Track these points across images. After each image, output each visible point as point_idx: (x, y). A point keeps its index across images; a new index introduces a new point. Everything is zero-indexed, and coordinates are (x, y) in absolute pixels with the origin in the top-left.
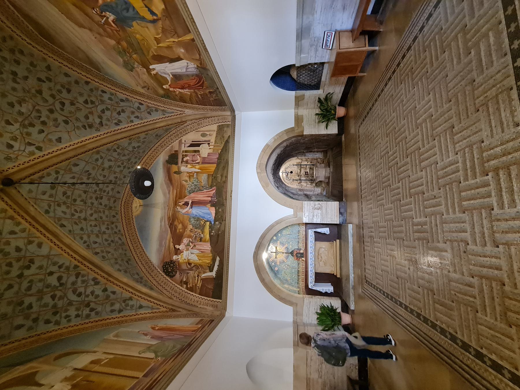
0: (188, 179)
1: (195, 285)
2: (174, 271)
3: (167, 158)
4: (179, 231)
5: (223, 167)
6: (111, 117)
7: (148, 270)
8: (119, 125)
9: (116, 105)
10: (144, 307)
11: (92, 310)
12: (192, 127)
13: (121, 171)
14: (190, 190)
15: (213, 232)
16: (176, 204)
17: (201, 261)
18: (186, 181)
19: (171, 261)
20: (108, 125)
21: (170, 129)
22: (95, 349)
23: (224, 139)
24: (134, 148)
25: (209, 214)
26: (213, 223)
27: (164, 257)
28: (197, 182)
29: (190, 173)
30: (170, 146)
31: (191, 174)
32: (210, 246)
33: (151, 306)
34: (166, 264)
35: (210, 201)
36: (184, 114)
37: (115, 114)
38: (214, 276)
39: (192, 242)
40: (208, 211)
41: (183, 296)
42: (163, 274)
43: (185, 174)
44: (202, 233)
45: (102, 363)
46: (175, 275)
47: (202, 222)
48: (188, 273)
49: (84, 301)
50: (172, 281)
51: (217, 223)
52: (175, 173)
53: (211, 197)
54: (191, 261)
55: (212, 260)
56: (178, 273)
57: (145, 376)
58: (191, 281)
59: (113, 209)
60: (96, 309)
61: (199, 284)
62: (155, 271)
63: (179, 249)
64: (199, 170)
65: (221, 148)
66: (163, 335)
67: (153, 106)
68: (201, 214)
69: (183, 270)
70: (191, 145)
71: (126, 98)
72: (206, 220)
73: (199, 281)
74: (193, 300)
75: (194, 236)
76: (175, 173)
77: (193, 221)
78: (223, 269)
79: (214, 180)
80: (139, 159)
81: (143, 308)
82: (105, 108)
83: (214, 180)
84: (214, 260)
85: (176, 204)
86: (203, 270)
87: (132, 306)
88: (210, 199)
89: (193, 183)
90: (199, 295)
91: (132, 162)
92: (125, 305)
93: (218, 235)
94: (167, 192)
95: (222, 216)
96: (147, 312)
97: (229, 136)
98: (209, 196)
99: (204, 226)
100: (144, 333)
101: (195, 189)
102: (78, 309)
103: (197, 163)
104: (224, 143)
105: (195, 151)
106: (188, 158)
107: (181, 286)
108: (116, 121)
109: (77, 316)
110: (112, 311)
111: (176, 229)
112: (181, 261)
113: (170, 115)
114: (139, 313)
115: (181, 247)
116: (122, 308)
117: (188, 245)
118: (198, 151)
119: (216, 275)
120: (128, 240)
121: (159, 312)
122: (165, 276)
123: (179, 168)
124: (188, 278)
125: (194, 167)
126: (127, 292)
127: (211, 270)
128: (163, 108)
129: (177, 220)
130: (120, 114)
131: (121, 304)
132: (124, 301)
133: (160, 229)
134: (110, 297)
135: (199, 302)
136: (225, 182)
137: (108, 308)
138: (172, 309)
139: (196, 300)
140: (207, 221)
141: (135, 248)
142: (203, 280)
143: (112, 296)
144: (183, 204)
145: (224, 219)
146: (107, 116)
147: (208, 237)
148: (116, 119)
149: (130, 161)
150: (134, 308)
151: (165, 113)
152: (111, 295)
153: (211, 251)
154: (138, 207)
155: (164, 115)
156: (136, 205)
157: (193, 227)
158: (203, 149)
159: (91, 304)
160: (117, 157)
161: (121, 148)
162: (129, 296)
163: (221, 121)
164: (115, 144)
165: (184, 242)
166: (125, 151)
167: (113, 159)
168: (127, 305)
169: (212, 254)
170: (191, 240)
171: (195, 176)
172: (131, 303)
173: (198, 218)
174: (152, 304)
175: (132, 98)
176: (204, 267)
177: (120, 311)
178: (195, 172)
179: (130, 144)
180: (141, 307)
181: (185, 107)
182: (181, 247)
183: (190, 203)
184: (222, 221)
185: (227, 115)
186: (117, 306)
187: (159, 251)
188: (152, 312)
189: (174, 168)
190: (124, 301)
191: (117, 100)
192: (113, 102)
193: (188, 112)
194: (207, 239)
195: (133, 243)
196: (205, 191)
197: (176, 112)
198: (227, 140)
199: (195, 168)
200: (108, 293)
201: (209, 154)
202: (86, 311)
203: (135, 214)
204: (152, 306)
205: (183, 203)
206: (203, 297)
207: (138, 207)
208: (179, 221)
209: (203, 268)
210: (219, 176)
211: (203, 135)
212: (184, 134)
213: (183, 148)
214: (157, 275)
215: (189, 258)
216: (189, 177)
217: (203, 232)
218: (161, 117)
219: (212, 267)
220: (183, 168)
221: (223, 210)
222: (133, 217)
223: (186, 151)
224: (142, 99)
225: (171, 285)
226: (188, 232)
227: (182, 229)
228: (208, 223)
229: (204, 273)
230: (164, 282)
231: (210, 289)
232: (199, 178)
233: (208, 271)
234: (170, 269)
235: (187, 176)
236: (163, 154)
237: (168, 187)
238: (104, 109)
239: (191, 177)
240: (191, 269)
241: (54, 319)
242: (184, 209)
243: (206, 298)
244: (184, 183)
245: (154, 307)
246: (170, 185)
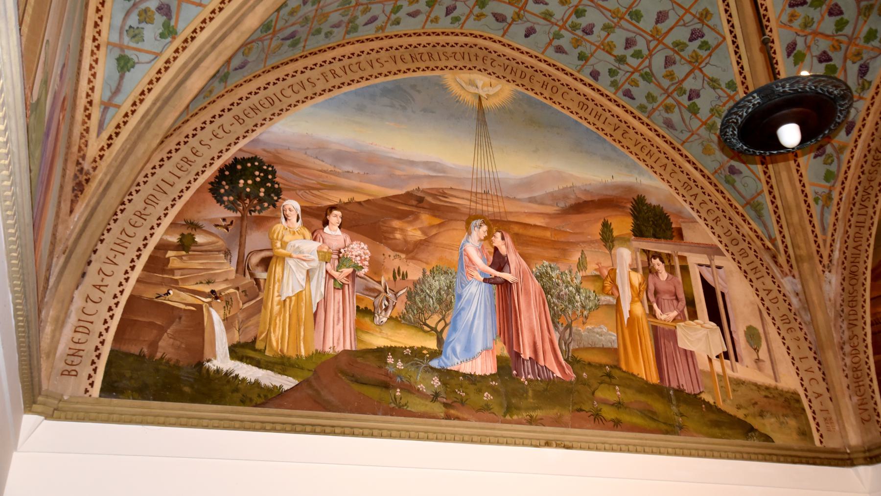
0: (591, 270)
1: (176, 281)
2: (239, 198)
3: (652, 201)
4: (395, 229)
5: (654, 413)
6: (815, 33)
7: (245, 104)
8: (789, 55)
9: (853, 49)
10: (122, 77)
12: (772, 295)
13: (609, 49)
14: (551, 278)
15: (400, 365)
16: (496, 224)
17: (276, 308)
18: (582, 265)
19: (278, 192)
20: (791, 21)
21: (760, 216)
23: (754, 416)
24: (694, 95)
25: (468, 347)
26: (435, 363)
27: (298, 166)
28: (584, 307)
29: (613, 281)
30: (695, 215)
31: (608, 284)
32: (340, 349)
33: (117, 100)
34: (266, 172)
35: (518, 355)
36: (820, 268)
37: (823, 45)
38: (213, 365)
39: (353, 276)
40: (479, 347)
41: (130, 230)
42: (227, 157)
43: (606, 263)
44: (391, 318)
46: (220, 201)
47: (436, 318)
48: (227, 253)
50: (198, 191)
51: (436, 382)
52: (606, 226)
53: (534, 361)
54: (279, 269)
55: (283, 357)
56: (230, 214)
58: (195, 264)
59: (477, 10)
61: (178, 299)
62: (240, 130)
63: (326, 223)
64: (626, 315)
65: (721, 405)
67: (844, 167)
68: (467, 316)
69: (242, 237)
70: (709, 290)
71: (870, 83)
72: (444, 336)
73: (190, 299)
74: (108, 269)
75: (377, 287)
76: (606, 226)
77: (436, 284)
78: (243, 402)
79: (599, 373)
80: (642, 108)
81: (117, 75)
82: (846, 16)
83: (599, 373)
84: (281, 365)
85: (496, 224)
86: (241, 316)
87: (136, 34)
88: (527, 353)
89: (578, 290)
90: (131, 298)
91: (637, 85)
92: (146, 11)
93: (386, 386)
94: (535, 194)
95: (462, 402)
96: (98, 83)
97: (768, 438)
98: (535, 351)
99: (419, 325)
101: (559, 297)
103: (651, 308)
104: (740, 414)
105: (691, 303)
106: (664, 275)
107: (173, 224)
108: (800, 46)
111: (402, 216)
112: (279, 228)
113: (816, 221)
114: (101, 54)
115: (334, 233)
117: (342, 260)
118: (693, 316)
119: (218, 371)
120: (358, 45)
121: (87, 130)
122: (218, 164)
123: (624, 241)
124: (206, 251)
125: (637, 295)
126: (197, 23)
127: (237, 352)
128: (835, 196)
129: (437, 221)
130: (820, 61)
133: (400, 161)
135: (96, 294)
136: (597, 419)
138: (87, 181)
139: (107, 281)
140: (440, 341)
141: (327, 67)
142: (197, 316)
144: (496, 249)
145: (452, 412)
146: (819, 22)
147: (378, 341)
148: (809, 47)
149: (640, 79)
150: (126, 40)
151: (820, 203)
153: (319, 354)
154: (472, 90)
155: (816, 200)
156: (480, 84)
157: (415, 284)
158: (704, 332)
160: (669, 40)
161: (703, 53)
162: (180, 27)
163: (816, 405)
164: (724, 38)
165: (355, 245)
166: (687, 68)
167: (663, 27)
168: (145, 16)
169: (309, 358)
170: (362, 273)
171: (605, 299)
172: (151, 32)
173: (449, 306)
174: (126, 107)
175: (868, 103)
176: (253, 321)
178: (618, 300)
179: (714, 83)
180: (124, 64)
181: (851, 277)
182: (334, 233)
183: (504, 275)
184: (446, 405)
185: (843, 428)
187: (320, 149)
188: (90, 103)
189: (622, 225)
191: (865, 56)
192: (861, 42)
193: (832, 283)
194: (366, 338)
195: (346, 61)
196: (556, 337)
197: (825, 241)
198: (752, 429)
199: (633, 302)
201: (689, 355)
203: (448, 77)
205: (503, 250)
206: (118, 312)
207: (472, 90)
208: (434, 232)
209: (248, 317)
210: (615, 394)
211: (752, 335)
212: (744, 267)
213: (694, 259)
214: (221, 133)
215: (290, 262)
216: (598, 278)
217: (396, 321)
218: (808, 189)
219: (251, 354)
220: (625, 255)
221: (486, 408)
222: (437, 73)
223: (685, 269)
224: (865, 133)
225: (182, 185)
226: (394, 261)
227: (406, 241)
228: (432, 344)
229: (225, 320)
230: (192, 157)
231: (154, 345)
232: (600, 313)
233: (237, 338)
234: (246, 183)
235: (599, 270)
236: (664, 186)
237: (554, 198)
238: (841, 13)
239: (598, 284)
240: (243, 267)
242: (481, 250)
243: (114, 325)
244: (576, 257)
245: (112, 110)
246: (562, 205)
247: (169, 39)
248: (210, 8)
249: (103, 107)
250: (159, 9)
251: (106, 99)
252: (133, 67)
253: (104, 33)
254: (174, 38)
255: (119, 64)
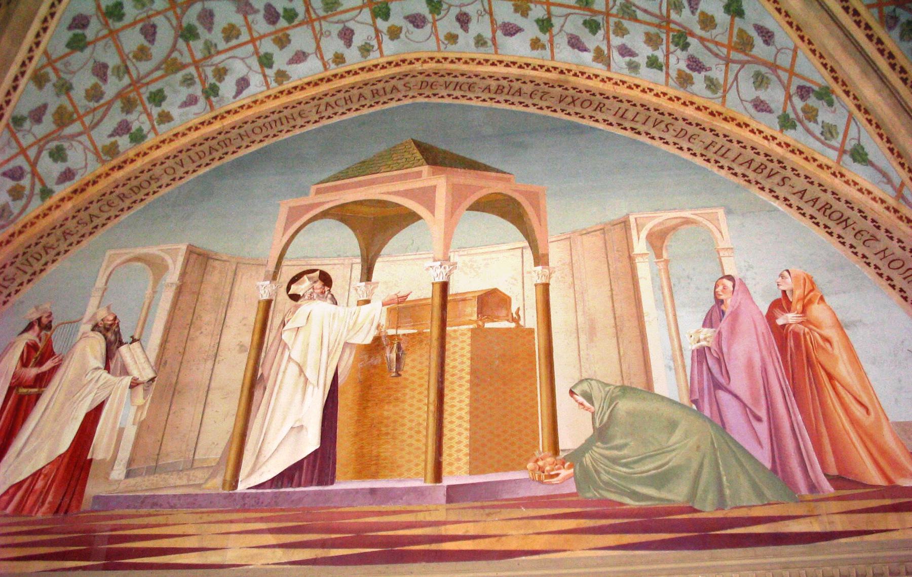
10: (872, 164)
11: (696, 65)
22: (556, 253)
45: (488, 325)
49: (668, 20)
57: (454, 494)
60: (710, 69)
66: (739, 383)
87: (829, 131)
92: (804, 110)
96: (877, 193)
100: (719, 302)
102: (652, 40)
109: (653, 63)
110: (760, 106)
116: (792, 116)
131: (789, 97)
132: (804, 92)
134: (752, 46)
137: (748, 91)
143: (760, 49)
150: (836, 143)
152: (758, 41)
159: (690, 39)
168: (811, 114)
172: (825, 115)
177: (786, 123)
180: (859, 155)
186: (774, 95)
190: (804, 92)
200: (746, 25)
202: (678, 62)
204: (903, 184)
241: (594, 41)
245: (905, 192)
247: (834, 97)
248: (798, 41)
249: (901, 200)
250: (802, 97)
251: (894, 194)
252: (863, 149)
253: (830, 164)
254: (833, 92)
255: (859, 162)
